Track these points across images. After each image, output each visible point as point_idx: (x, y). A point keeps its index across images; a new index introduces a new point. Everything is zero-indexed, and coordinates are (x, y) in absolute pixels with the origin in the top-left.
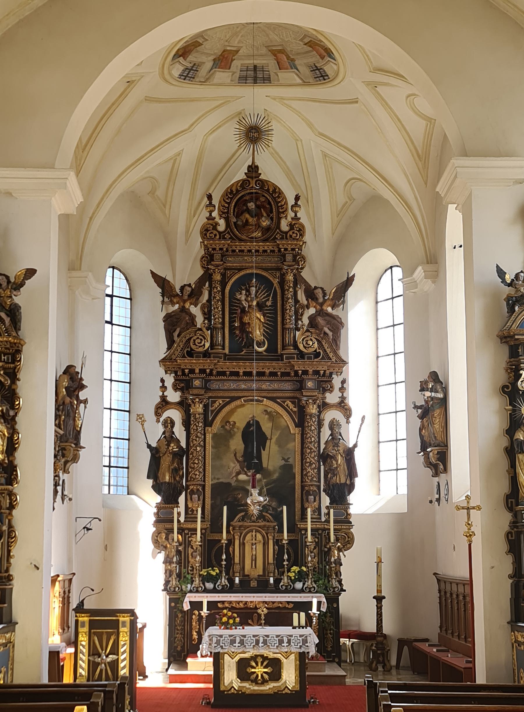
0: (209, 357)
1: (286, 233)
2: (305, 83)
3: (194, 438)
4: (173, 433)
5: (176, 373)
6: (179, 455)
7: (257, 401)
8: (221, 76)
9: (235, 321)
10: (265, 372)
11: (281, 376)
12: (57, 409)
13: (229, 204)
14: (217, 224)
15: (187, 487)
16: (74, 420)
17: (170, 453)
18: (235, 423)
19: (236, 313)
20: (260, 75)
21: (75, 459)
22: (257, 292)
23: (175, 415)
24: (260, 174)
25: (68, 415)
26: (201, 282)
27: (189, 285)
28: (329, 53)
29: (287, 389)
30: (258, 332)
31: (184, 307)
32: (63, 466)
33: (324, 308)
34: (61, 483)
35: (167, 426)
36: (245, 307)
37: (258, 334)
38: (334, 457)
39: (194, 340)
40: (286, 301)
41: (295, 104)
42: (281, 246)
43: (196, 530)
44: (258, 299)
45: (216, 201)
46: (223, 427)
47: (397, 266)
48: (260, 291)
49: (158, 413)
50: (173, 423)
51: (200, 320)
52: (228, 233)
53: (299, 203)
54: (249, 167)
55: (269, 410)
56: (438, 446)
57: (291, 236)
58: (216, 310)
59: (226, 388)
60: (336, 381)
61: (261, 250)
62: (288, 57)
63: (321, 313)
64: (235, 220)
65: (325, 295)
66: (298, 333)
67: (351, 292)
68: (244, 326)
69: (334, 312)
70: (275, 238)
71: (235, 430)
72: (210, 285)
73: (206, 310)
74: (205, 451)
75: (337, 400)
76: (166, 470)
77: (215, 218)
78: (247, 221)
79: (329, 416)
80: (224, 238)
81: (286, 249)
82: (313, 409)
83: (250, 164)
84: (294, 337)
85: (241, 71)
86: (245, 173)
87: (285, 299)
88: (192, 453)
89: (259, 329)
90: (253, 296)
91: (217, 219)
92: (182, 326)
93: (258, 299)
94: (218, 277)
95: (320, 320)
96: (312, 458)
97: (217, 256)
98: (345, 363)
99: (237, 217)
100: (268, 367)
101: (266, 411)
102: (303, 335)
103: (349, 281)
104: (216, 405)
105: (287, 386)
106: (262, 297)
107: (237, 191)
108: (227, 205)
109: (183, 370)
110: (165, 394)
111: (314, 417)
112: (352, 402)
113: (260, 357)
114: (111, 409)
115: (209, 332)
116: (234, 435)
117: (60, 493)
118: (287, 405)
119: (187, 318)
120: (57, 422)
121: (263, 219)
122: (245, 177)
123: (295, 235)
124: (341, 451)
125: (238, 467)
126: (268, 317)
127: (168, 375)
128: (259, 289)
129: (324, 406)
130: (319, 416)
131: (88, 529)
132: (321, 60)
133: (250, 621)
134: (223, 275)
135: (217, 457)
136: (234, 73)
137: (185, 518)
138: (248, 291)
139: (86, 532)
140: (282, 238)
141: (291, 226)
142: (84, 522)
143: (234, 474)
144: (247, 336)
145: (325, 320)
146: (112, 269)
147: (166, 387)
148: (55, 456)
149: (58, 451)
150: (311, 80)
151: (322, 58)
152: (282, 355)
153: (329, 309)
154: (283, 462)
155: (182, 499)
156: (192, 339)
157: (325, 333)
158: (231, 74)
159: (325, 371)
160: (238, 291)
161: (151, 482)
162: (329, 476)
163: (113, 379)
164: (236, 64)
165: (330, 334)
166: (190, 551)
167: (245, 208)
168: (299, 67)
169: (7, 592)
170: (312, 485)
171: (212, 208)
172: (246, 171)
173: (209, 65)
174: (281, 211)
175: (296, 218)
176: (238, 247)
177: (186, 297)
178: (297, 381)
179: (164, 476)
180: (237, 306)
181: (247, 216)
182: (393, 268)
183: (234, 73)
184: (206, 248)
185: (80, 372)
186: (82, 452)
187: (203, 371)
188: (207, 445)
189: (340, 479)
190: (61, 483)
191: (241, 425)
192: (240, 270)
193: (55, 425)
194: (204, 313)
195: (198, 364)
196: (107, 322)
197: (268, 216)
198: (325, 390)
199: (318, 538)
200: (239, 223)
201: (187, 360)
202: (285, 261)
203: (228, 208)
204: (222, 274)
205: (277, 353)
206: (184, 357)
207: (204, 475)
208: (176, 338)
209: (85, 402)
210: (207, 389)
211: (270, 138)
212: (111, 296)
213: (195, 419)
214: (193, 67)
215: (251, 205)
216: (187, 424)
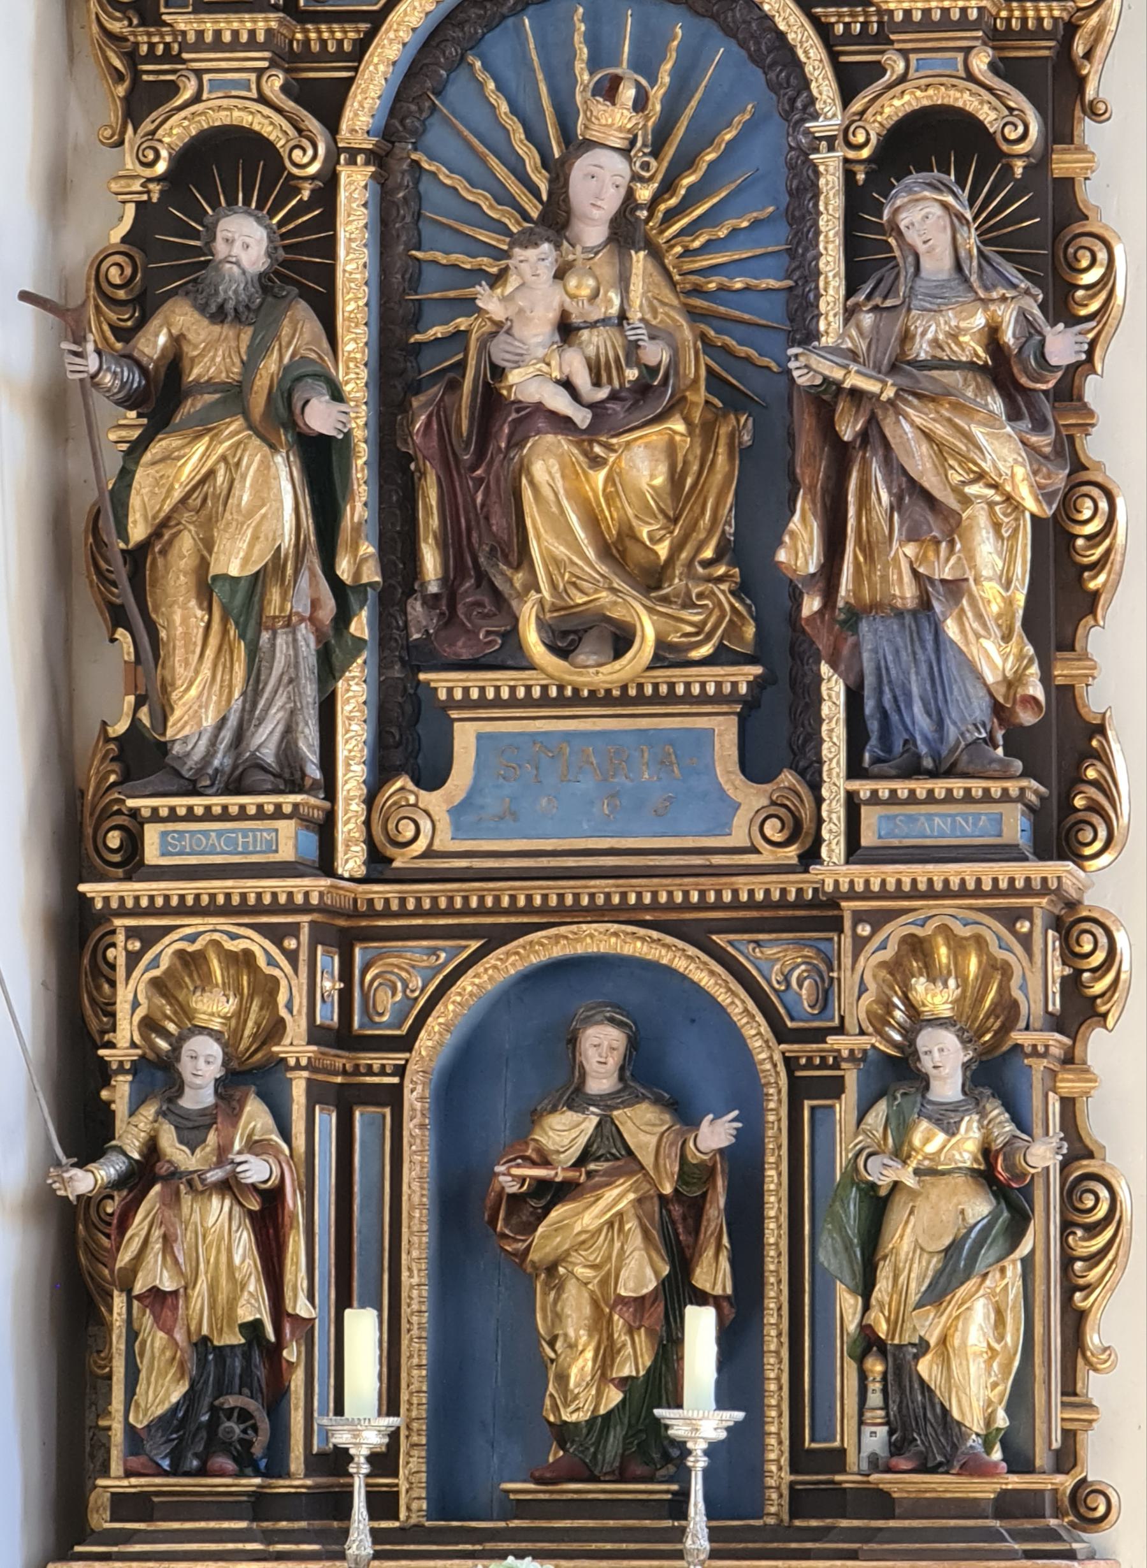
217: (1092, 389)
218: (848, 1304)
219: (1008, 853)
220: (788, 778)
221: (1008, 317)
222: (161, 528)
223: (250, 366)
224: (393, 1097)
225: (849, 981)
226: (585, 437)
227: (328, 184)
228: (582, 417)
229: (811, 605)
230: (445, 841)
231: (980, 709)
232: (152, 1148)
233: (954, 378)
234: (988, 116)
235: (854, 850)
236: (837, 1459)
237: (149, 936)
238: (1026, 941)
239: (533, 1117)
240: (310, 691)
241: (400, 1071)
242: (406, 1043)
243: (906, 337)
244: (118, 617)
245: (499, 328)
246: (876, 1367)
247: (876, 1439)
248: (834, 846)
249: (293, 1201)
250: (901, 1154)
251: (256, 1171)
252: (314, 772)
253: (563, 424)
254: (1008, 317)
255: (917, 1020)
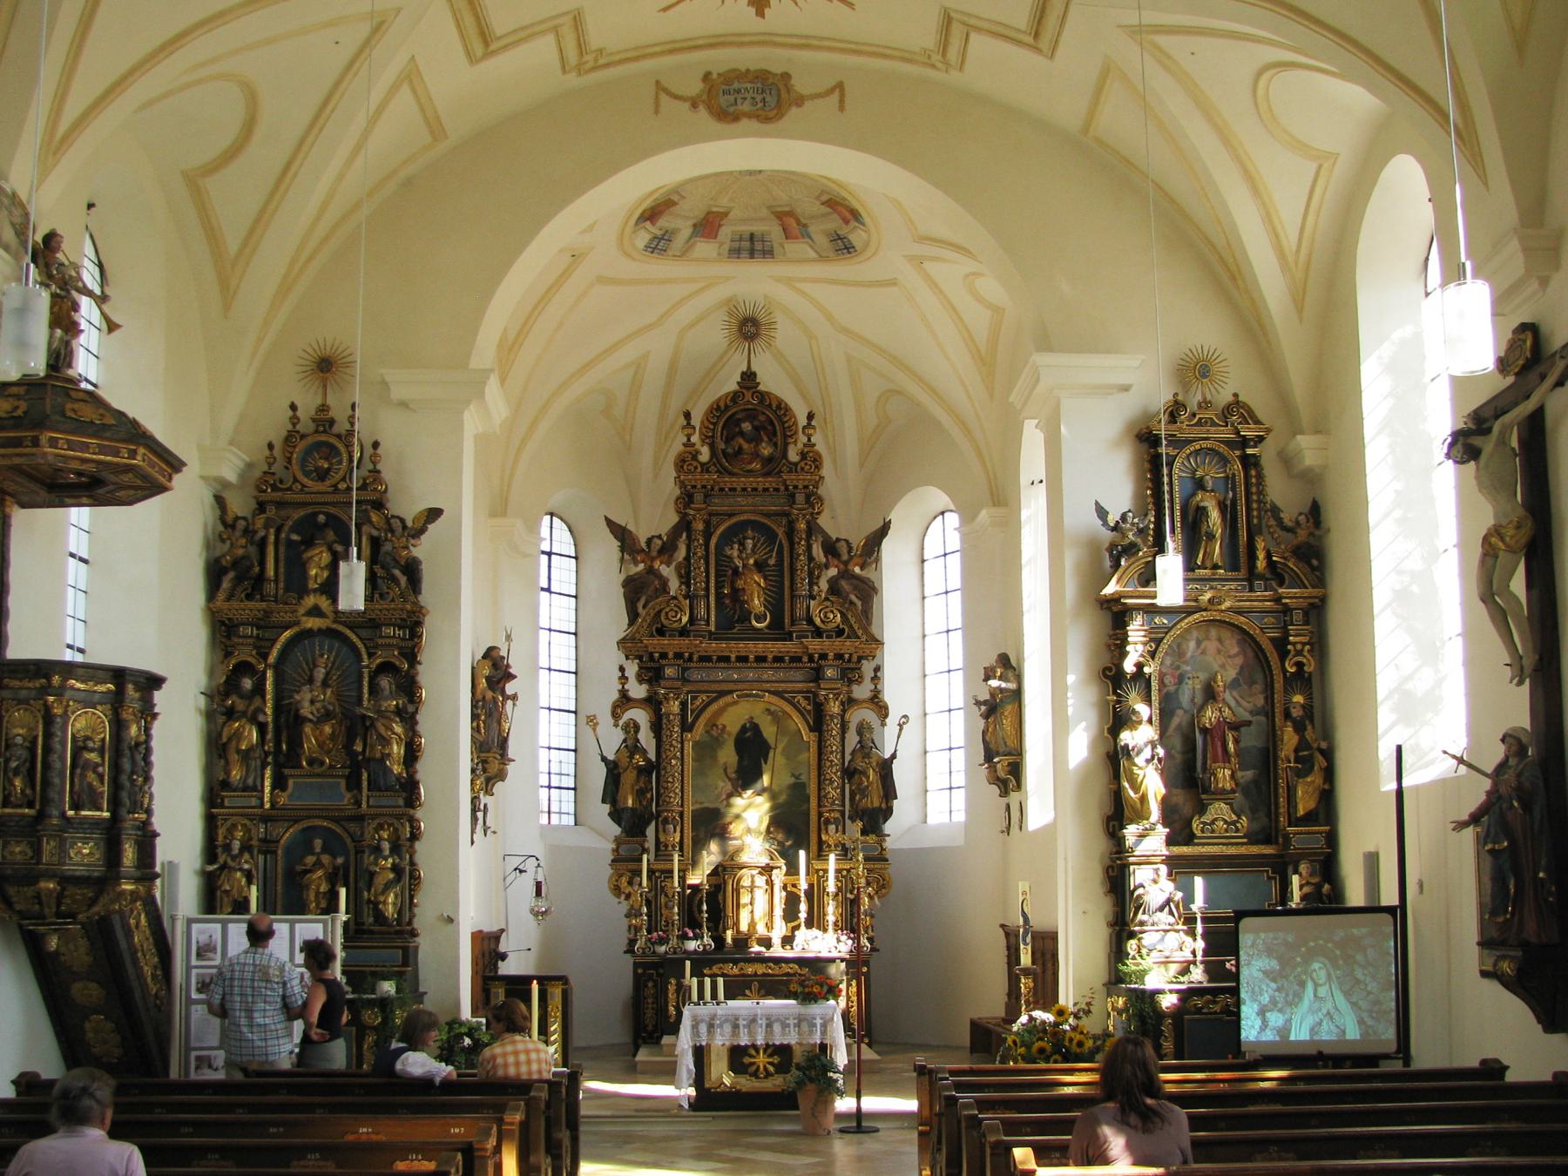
0: (688, 636)
1: (796, 464)
2: (822, 258)
3: (667, 747)
4: (638, 741)
5: (640, 658)
6: (646, 771)
7: (756, 696)
8: (704, 248)
9: (724, 586)
10: (766, 657)
11: (790, 662)
12: (474, 706)
13: (714, 424)
14: (698, 452)
15: (659, 813)
16: (499, 723)
17: (634, 768)
18: (725, 727)
19: (725, 576)
20: (758, 246)
21: (501, 776)
22: (754, 546)
23: (641, 716)
24: (759, 383)
25: (489, 715)
26: (675, 532)
27: (659, 537)
28: (855, 215)
29: (797, 679)
30: (757, 602)
31: (651, 567)
32: (484, 785)
33: (850, 567)
34: (482, 807)
35: (629, 732)
36: (737, 567)
37: (757, 604)
38: (864, 773)
39: (667, 613)
40: (797, 559)
41: (807, 287)
42: (788, 482)
43: (671, 871)
44: (757, 556)
45: (696, 421)
46: (707, 732)
47: (951, 511)
48: (759, 545)
49: (616, 716)
50: (637, 728)
51: (674, 585)
52: (714, 464)
53: (813, 423)
54: (743, 373)
55: (773, 708)
56: (1009, 754)
57: (802, 469)
58: (697, 571)
59: (712, 678)
60: (867, 668)
61: (760, 488)
62: (799, 222)
63: (845, 574)
64: (723, 446)
65: (850, 549)
66: (812, 602)
67: (887, 545)
68: (736, 593)
69: (864, 574)
70: (781, 471)
71: (726, 736)
72: (689, 537)
73: (683, 572)
74: (682, 765)
75: (868, 695)
76: (629, 791)
77: (694, 444)
78: (740, 448)
79: (856, 716)
80: (708, 471)
81: (796, 487)
82: (835, 708)
83: (745, 370)
84: (808, 607)
85: (732, 241)
86: (738, 383)
87: (795, 556)
88: (665, 768)
89: (759, 597)
90: (749, 551)
91: (698, 446)
92: (649, 593)
93: (757, 556)
94: (699, 526)
95: (844, 584)
96: (834, 774)
97: (699, 497)
98: (880, 643)
99: (728, 441)
100: (772, 648)
101: (768, 710)
102: (820, 605)
103: (884, 530)
104: (698, 702)
105: (799, 675)
106: (761, 555)
107: (727, 407)
108: (712, 427)
109: (651, 655)
110: (626, 687)
111: (836, 718)
112: (888, 696)
113: (757, 635)
114: (550, 709)
115: (688, 601)
116: (723, 743)
117: (480, 822)
118: (798, 702)
119: (656, 582)
120: (475, 724)
121: (764, 445)
122: (738, 388)
123: (808, 467)
124: (874, 764)
125: (729, 787)
126: (771, 580)
127: (630, 661)
128: (758, 542)
129: (850, 702)
130: (843, 717)
131: (521, 871)
132: (844, 226)
133: (747, 992)
134: (707, 523)
135: (699, 772)
136: (721, 244)
137: (656, 856)
138: (742, 544)
139: (518, 874)
140: (790, 471)
141: (803, 455)
142: (515, 862)
143: (724, 797)
144: (742, 607)
145: (852, 584)
146: (549, 517)
147: (627, 678)
148: (473, 771)
149: (477, 764)
150: (831, 254)
151: (847, 222)
152: (790, 634)
153: (857, 570)
154: (792, 780)
155: (650, 831)
156: (664, 612)
157: (852, 603)
158: (717, 245)
159: (851, 655)
160: (727, 545)
161: (607, 808)
162: (857, 798)
163: (552, 667)
164: (726, 232)
165: (859, 603)
166: (663, 899)
167: (737, 430)
168: (813, 236)
169: (411, 951)
170: (833, 810)
171: (690, 431)
172: (739, 380)
173: (686, 232)
174: (789, 434)
175: (810, 444)
176: (729, 485)
177: (654, 554)
178: (812, 669)
179: (626, 799)
180: (726, 566)
181: (741, 441)
182: (946, 514)
183: (721, 244)
184: (682, 485)
185: (506, 656)
186: (510, 768)
187: (679, 656)
188: (685, 757)
189: (872, 803)
190: (482, 807)
191: (733, 728)
192: (731, 515)
193: (472, 728)
194: (680, 576)
195: (671, 644)
196: (543, 589)
197: (770, 440)
198: (850, 682)
199: (841, 881)
200: (730, 450)
201: (656, 641)
202: (794, 503)
203: (713, 430)
204: (704, 521)
205: (783, 628)
206: (652, 636)
207: (682, 797)
208: (640, 609)
209: (514, 697)
210: (685, 680)
211: (772, 334)
212: (549, 554)
213: (669, 721)
214: (664, 235)
215: (747, 426)
216: (657, 728)
217: (418, 717)
218: (366, 894)
219: (400, 807)
220: (355, 791)
221: (401, 702)
222: (230, 739)
223: (248, 707)
224: (275, 853)
225: (366, 832)
226: (315, 723)
227: (264, 673)
228: (315, 719)
229: (360, 758)
230: (287, 802)
231: (394, 779)
232: (225, 862)
233: (389, 714)
234: (397, 663)
235: (368, 806)
236: (363, 924)
237: (225, 820)
238: (402, 824)
239: (303, 857)
240: (259, 772)
241: (277, 847)
242: (278, 841)
243: (380, 706)
244: (220, 757)
245: (299, 702)
246: (371, 906)
247: (371, 920)
248: (364, 805)
249: (254, 872)
250: (377, 865)
251: (246, 866)
252: (260, 788)
253: (311, 721)
254: (401, 702)
255: (381, 839)
